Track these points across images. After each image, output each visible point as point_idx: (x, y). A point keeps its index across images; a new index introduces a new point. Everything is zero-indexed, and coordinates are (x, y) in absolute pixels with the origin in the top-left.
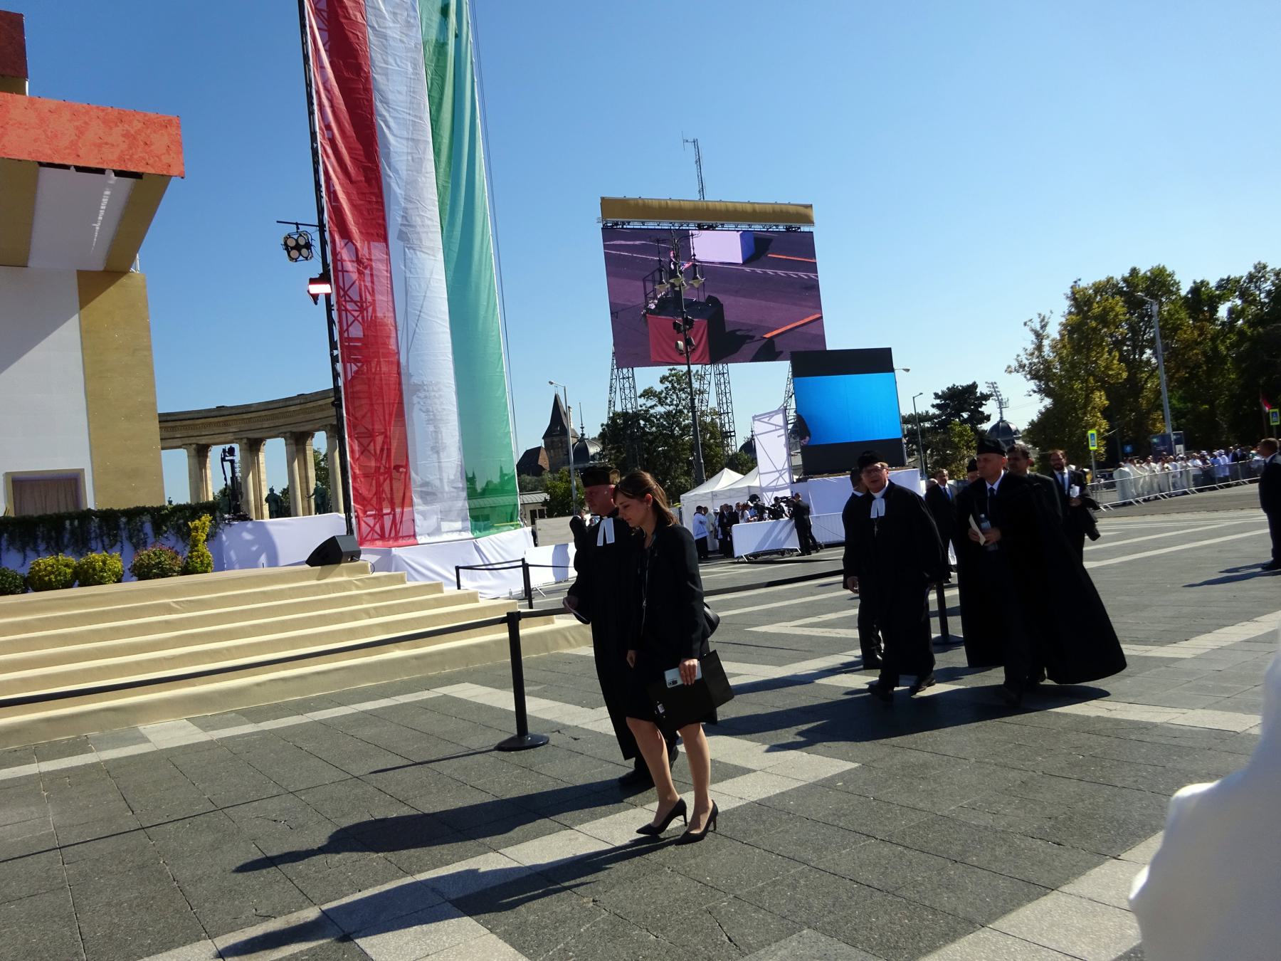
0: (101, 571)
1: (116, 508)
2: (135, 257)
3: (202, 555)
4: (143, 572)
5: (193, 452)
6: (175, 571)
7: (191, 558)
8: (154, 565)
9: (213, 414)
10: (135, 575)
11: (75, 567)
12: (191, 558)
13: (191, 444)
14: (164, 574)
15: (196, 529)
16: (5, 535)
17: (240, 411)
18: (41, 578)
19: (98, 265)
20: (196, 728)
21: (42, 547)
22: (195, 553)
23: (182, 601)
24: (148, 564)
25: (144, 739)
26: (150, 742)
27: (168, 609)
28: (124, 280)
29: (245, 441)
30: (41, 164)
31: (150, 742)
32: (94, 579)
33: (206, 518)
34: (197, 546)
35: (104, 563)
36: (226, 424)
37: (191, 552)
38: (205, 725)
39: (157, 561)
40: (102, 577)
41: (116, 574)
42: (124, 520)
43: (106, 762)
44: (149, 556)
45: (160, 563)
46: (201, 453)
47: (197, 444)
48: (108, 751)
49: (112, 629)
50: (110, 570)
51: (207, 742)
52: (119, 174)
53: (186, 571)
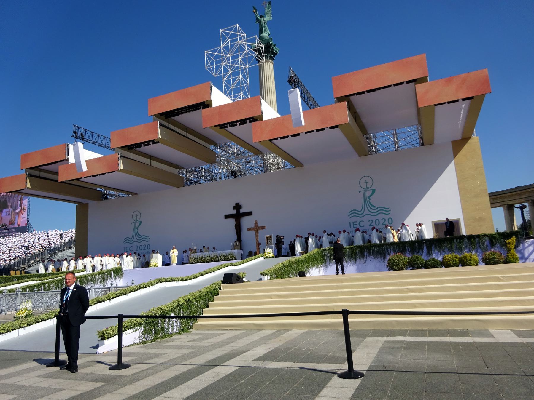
0: (470, 261)
1: (474, 234)
2: (473, 130)
3: (513, 255)
4: (487, 262)
5: (506, 208)
6: (501, 262)
7: (508, 256)
8: (491, 259)
9: (514, 190)
10: (484, 263)
11: (460, 258)
12: (508, 256)
13: (504, 205)
14: (497, 262)
15: (509, 243)
16: (433, 245)
17: (527, 188)
18: (447, 262)
19: (458, 136)
20: (515, 335)
21: (446, 250)
22: (510, 254)
23: (504, 276)
24: (489, 258)
25: (492, 336)
26: (494, 337)
27: (498, 279)
28: (470, 141)
29: (531, 201)
30: (435, 105)
31: (494, 337)
32: (467, 263)
33: (514, 239)
34: (510, 251)
35: (471, 257)
36: (520, 194)
37: (508, 253)
38: (520, 334)
39: (492, 257)
40: (470, 263)
41: (475, 262)
42: (477, 239)
43: (476, 342)
44: (489, 255)
45: (494, 258)
46: (510, 209)
47: (508, 205)
48: (477, 338)
49: (475, 286)
50: (473, 260)
51: (521, 343)
52: (464, 100)
53: (506, 262)
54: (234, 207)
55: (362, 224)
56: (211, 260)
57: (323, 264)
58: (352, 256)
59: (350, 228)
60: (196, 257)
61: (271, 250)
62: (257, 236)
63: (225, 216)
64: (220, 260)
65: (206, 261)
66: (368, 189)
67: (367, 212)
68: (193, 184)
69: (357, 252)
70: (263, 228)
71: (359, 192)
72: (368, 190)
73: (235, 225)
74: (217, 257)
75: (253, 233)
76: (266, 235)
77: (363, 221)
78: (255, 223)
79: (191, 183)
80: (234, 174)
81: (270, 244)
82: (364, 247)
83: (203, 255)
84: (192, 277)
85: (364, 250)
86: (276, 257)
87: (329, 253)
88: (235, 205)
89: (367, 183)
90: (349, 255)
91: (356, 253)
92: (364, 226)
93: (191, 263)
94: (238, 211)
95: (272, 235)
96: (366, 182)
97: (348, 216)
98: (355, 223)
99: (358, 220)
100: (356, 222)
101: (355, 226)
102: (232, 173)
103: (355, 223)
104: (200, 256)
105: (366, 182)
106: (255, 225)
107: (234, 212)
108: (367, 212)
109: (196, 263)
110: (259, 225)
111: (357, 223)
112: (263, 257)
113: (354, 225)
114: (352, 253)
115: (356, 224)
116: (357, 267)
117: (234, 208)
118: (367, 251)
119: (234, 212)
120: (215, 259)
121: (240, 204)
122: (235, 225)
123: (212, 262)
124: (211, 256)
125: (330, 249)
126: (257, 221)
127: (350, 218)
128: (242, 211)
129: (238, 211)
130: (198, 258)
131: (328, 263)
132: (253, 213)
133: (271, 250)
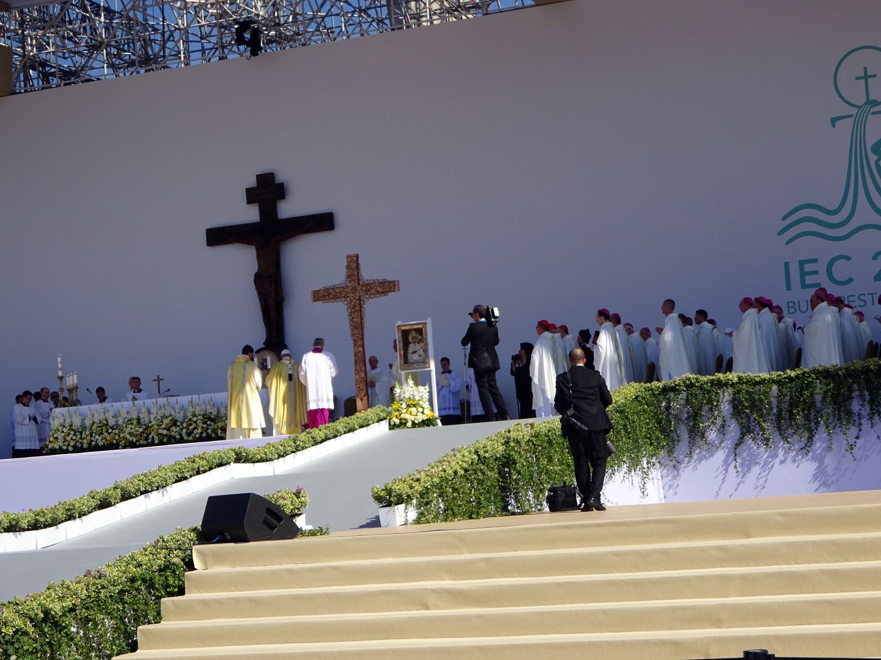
54: (248, 190)
55: (840, 270)
56: (147, 439)
57: (662, 453)
58: (792, 417)
59: (789, 288)
60: (77, 422)
61: (421, 388)
62: (358, 327)
63: (208, 230)
64: (189, 435)
65: (122, 443)
66: (873, 110)
67: (864, 214)
68: (54, 81)
69: (818, 398)
70: (387, 287)
71: (834, 121)
72: (873, 113)
73: (259, 279)
74: (174, 423)
75: (339, 309)
76: (399, 323)
77: (848, 258)
78: (348, 267)
79: (46, 77)
80: (247, 36)
81: (416, 362)
82: (851, 374)
83: (109, 416)
84: (61, 514)
85: (850, 390)
86: (447, 420)
87: (687, 400)
88: (252, 182)
89: (870, 80)
90: (780, 410)
91: (813, 403)
92: (850, 280)
93: (53, 452)
94: (268, 211)
95: (429, 321)
96: (866, 77)
97: (780, 233)
98: (808, 267)
99: (822, 250)
100: (816, 261)
101: (809, 280)
102: (240, 32)
103: (808, 267)
104: (96, 420)
105: (866, 77)
106: (349, 276)
107: (251, 214)
108: (864, 214)
109: (77, 449)
110: (368, 273)
111: (822, 267)
112: (384, 424)
113: (803, 274)
114: (793, 404)
115: (816, 273)
116: (814, 465)
117: (252, 196)
118: (861, 396)
119: (251, 214)
120: (165, 432)
121: (280, 178)
122: (255, 275)
123: (153, 444)
124: (145, 419)
125: (691, 385)
126: (357, 257)
127: (788, 243)
128: (287, 210)
129: (268, 211)
130: (84, 428)
131: (682, 447)
132: (341, 220)
133: (423, 391)
